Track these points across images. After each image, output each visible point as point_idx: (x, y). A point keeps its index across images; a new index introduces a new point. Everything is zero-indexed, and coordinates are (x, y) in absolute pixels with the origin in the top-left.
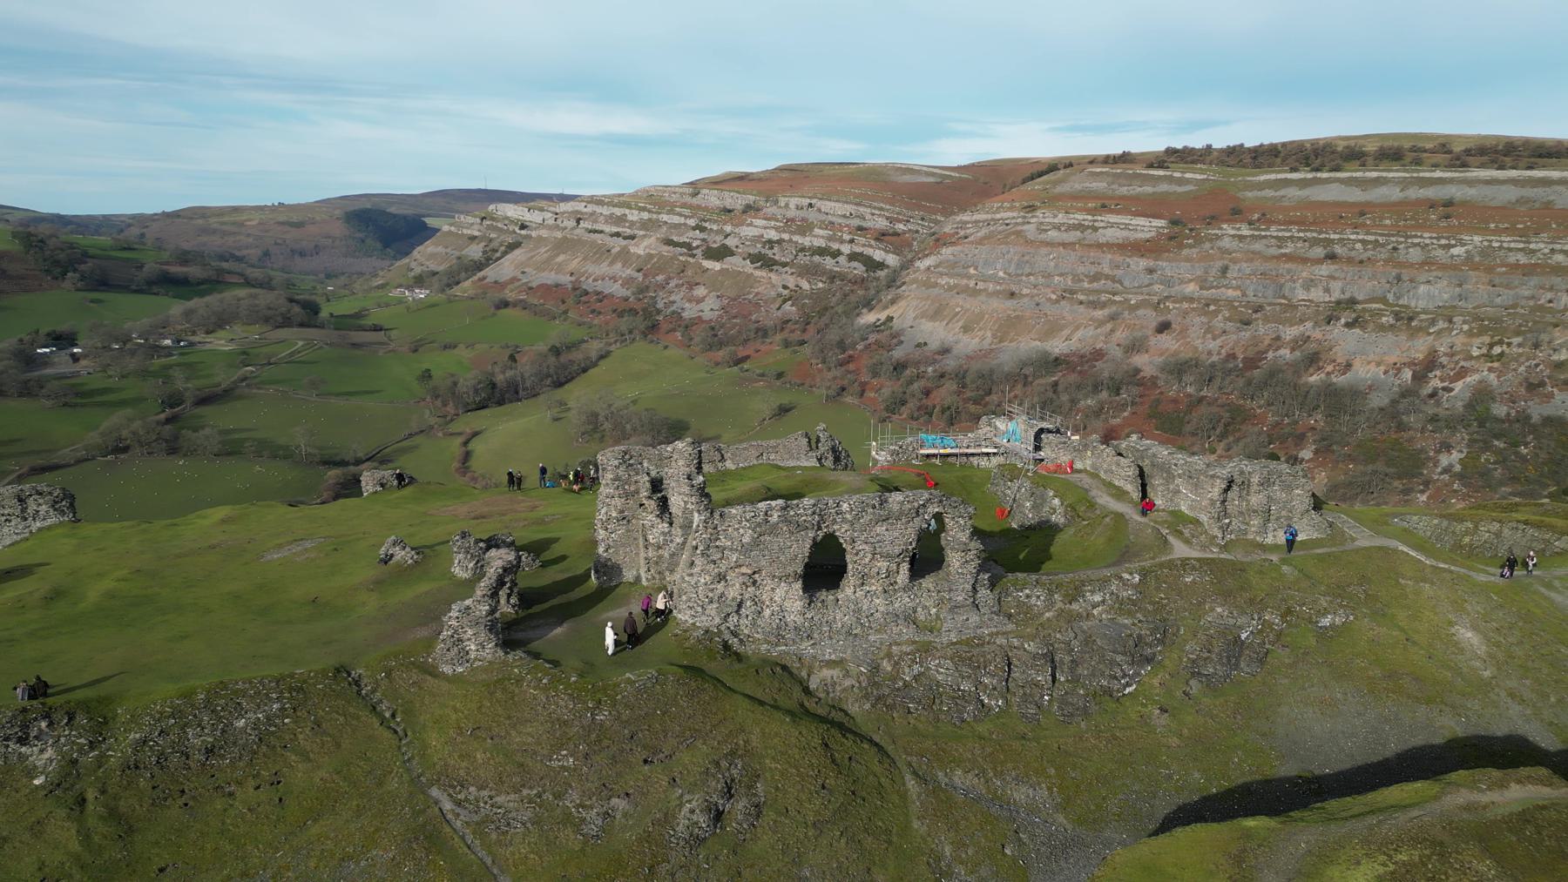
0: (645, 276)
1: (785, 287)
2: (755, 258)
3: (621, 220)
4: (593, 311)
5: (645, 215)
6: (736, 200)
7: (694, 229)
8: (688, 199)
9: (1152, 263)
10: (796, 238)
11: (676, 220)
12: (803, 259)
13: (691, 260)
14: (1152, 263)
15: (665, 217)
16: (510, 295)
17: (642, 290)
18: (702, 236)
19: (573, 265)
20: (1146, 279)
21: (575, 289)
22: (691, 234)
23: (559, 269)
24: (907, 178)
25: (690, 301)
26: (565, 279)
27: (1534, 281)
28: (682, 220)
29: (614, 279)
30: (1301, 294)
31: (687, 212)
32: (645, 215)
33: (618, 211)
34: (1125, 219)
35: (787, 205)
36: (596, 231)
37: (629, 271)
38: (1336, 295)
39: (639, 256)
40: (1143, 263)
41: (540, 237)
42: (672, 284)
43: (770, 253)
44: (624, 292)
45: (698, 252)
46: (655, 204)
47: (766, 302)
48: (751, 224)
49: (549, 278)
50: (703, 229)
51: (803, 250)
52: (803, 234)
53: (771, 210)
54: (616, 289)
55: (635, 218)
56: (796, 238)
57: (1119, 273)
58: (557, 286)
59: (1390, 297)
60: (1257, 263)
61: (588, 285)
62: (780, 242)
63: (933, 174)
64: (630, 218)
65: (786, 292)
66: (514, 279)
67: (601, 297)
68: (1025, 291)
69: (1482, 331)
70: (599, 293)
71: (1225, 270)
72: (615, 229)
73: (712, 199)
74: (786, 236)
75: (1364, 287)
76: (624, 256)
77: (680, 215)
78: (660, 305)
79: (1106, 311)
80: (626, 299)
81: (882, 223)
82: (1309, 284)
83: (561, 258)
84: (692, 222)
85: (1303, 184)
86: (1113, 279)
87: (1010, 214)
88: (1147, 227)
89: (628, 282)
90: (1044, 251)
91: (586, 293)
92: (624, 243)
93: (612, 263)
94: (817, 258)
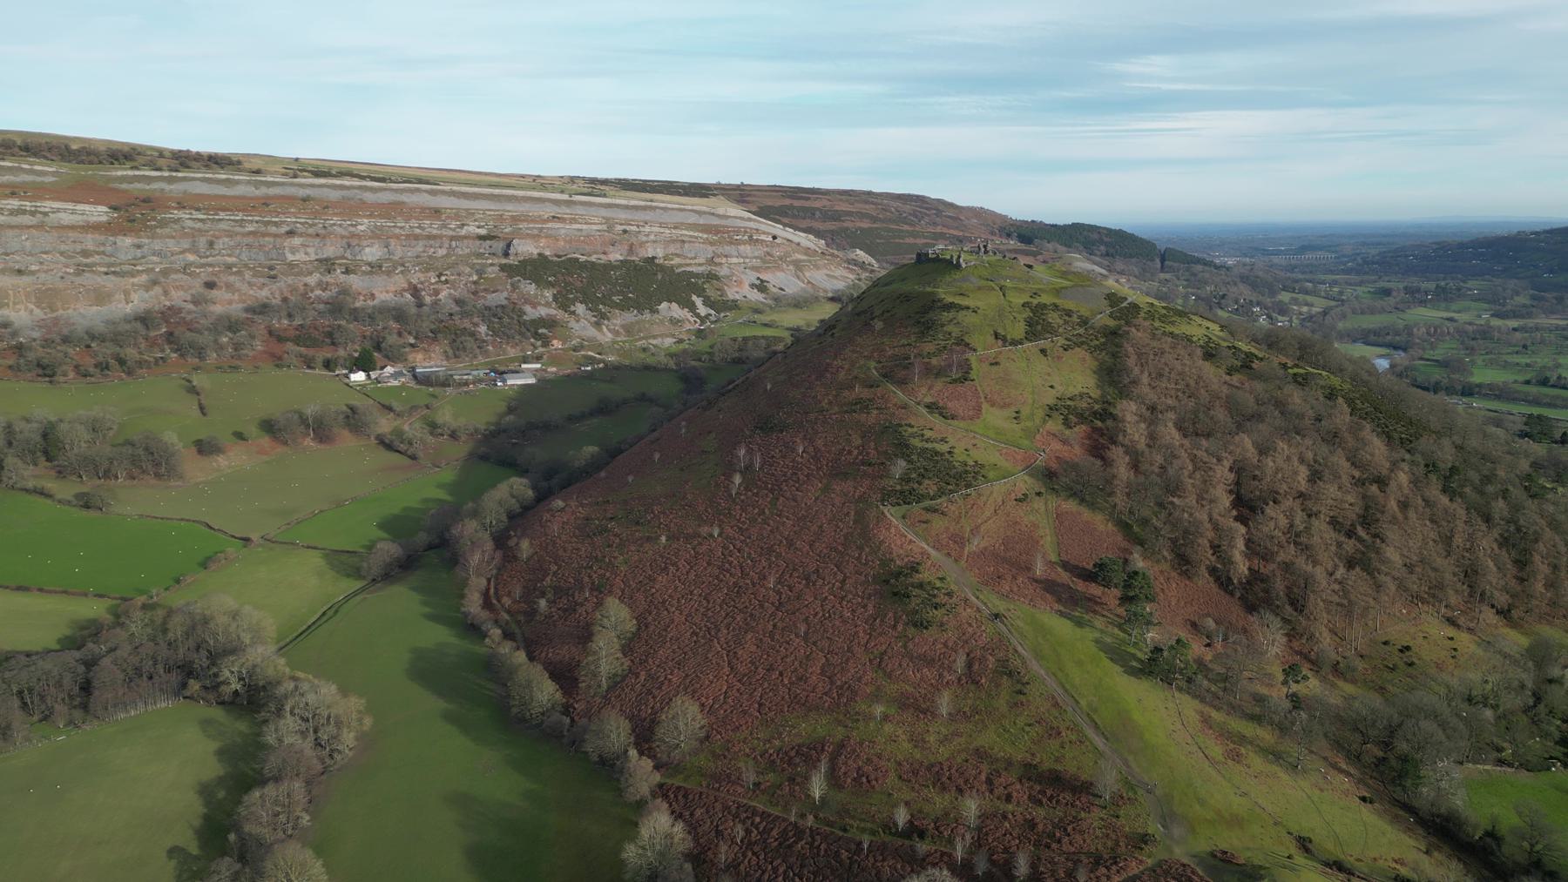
9: (136, 241)
14: (136, 241)
20: (139, 253)
27: (421, 243)
30: (290, 257)
34: (70, 206)
38: (313, 257)
40: (128, 241)
57: (109, 249)
59: (348, 255)
60: (239, 238)
68: (33, 268)
69: (428, 270)
71: (211, 244)
75: (330, 251)
79: (144, 278)
82: (294, 250)
85: (170, 180)
86: (103, 253)
88: (98, 213)
90: (10, 233)
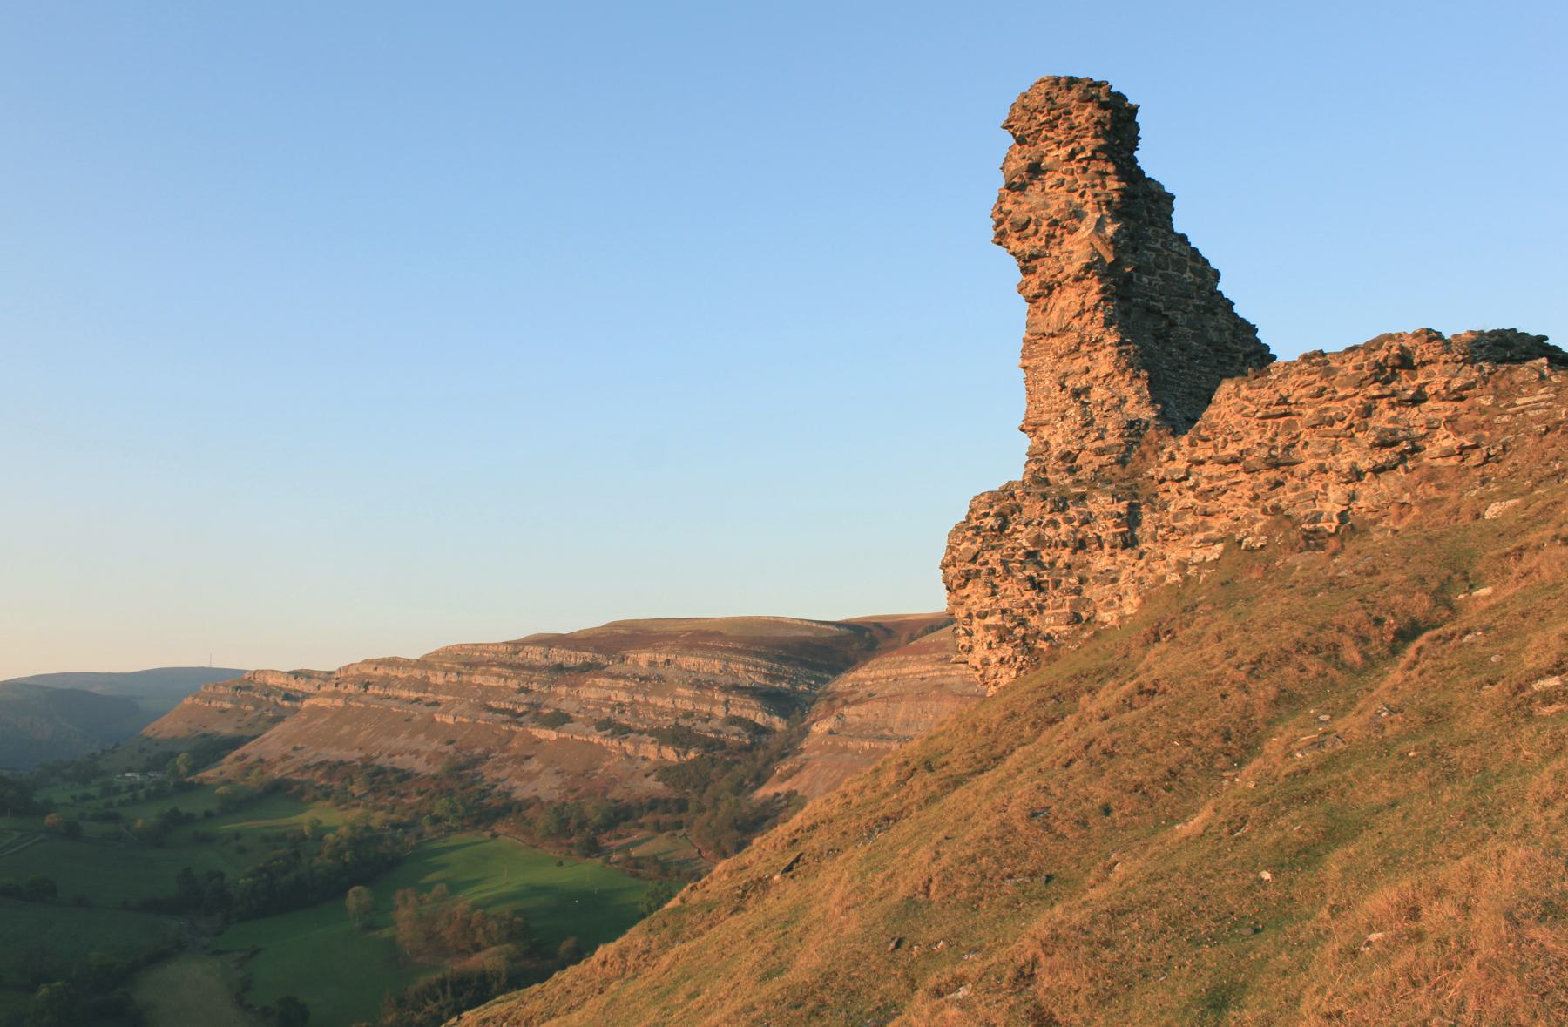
3: (424, 684)
6: (574, 659)
10: (652, 700)
13: (515, 728)
18: (529, 699)
24: (780, 633)
26: (353, 755)
29: (417, 753)
31: (508, 672)
32: (453, 678)
33: (417, 673)
37: (435, 745)
44: (434, 770)
46: (465, 664)
48: (594, 685)
53: (616, 668)
55: (440, 681)
58: (342, 763)
63: (810, 629)
64: (433, 679)
67: (405, 776)
70: (395, 770)
72: (414, 695)
76: (430, 727)
77: (500, 676)
84: (513, 684)
87: (922, 668)
92: (427, 710)
93: (412, 735)
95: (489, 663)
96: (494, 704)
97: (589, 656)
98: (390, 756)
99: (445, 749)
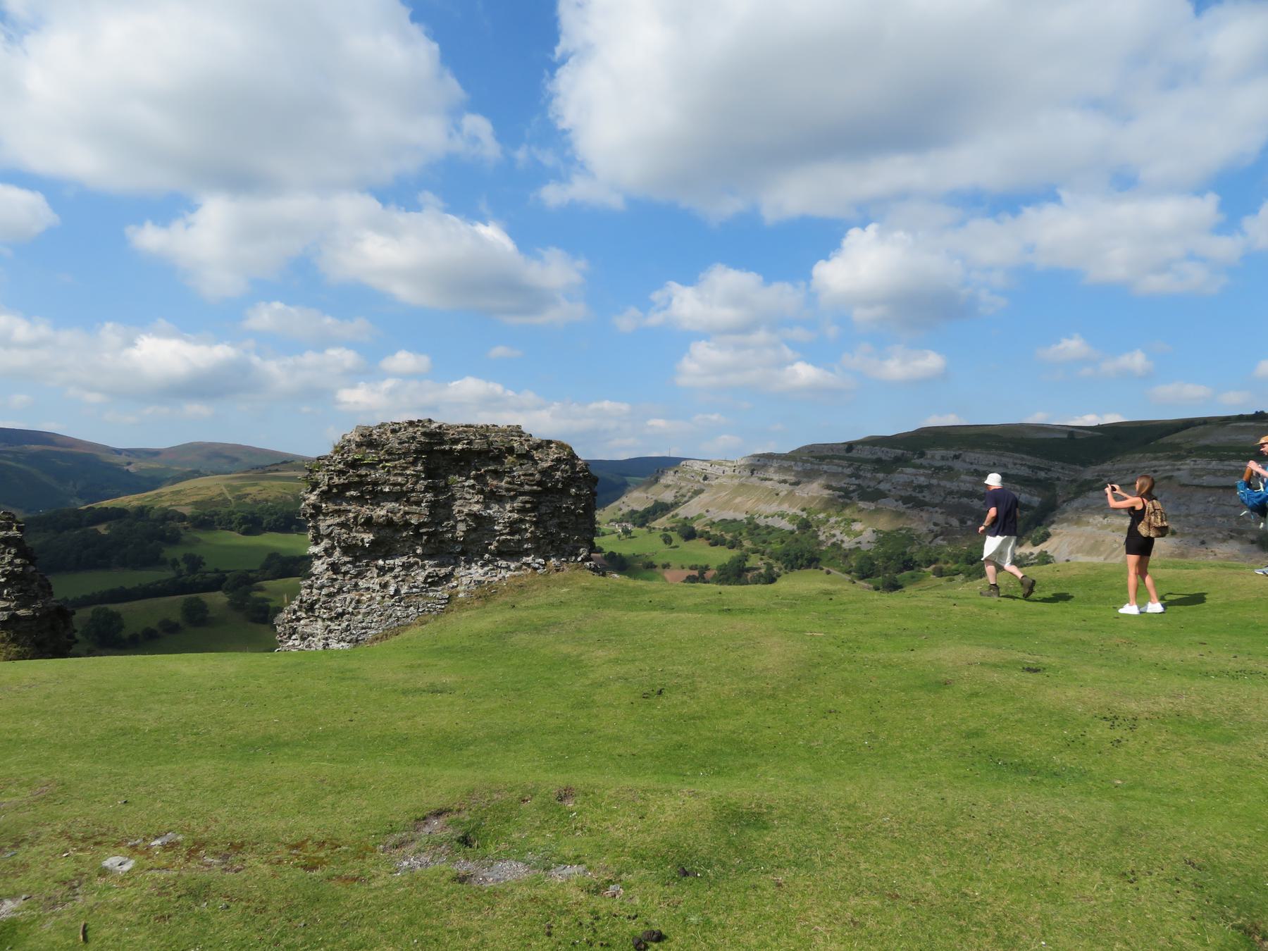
0: (809, 514)
1: (935, 524)
2: (906, 500)
4: (764, 542)
5: (808, 466)
6: (889, 454)
7: (850, 476)
8: (843, 454)
10: (943, 483)
11: (835, 469)
12: (951, 500)
15: (825, 468)
16: (698, 527)
17: (805, 525)
19: (749, 505)
21: (749, 523)
22: (847, 480)
23: (736, 509)
25: (848, 534)
26: (741, 516)
28: (840, 469)
29: (782, 516)
31: (845, 463)
32: (808, 466)
35: (933, 457)
36: (766, 479)
37: (794, 510)
39: (803, 498)
41: (721, 485)
42: (833, 520)
43: (920, 496)
45: (855, 495)
46: (816, 458)
47: (918, 536)
48: (902, 472)
49: (729, 515)
50: (858, 477)
51: (951, 493)
52: (951, 479)
54: (785, 525)
56: (943, 483)
58: (735, 520)
61: (761, 522)
62: (929, 487)
65: (936, 528)
66: (700, 516)
67: (770, 530)
70: (768, 527)
72: (782, 478)
73: (866, 453)
74: (934, 482)
77: (838, 465)
78: (822, 538)
80: (792, 532)
81: (1025, 472)
83: (738, 500)
84: (848, 471)
89: (793, 518)
91: (757, 527)
93: (780, 504)
94: (964, 500)
95: (832, 457)
96: (834, 484)
97: (899, 452)
98: (766, 517)
99: (800, 513)
